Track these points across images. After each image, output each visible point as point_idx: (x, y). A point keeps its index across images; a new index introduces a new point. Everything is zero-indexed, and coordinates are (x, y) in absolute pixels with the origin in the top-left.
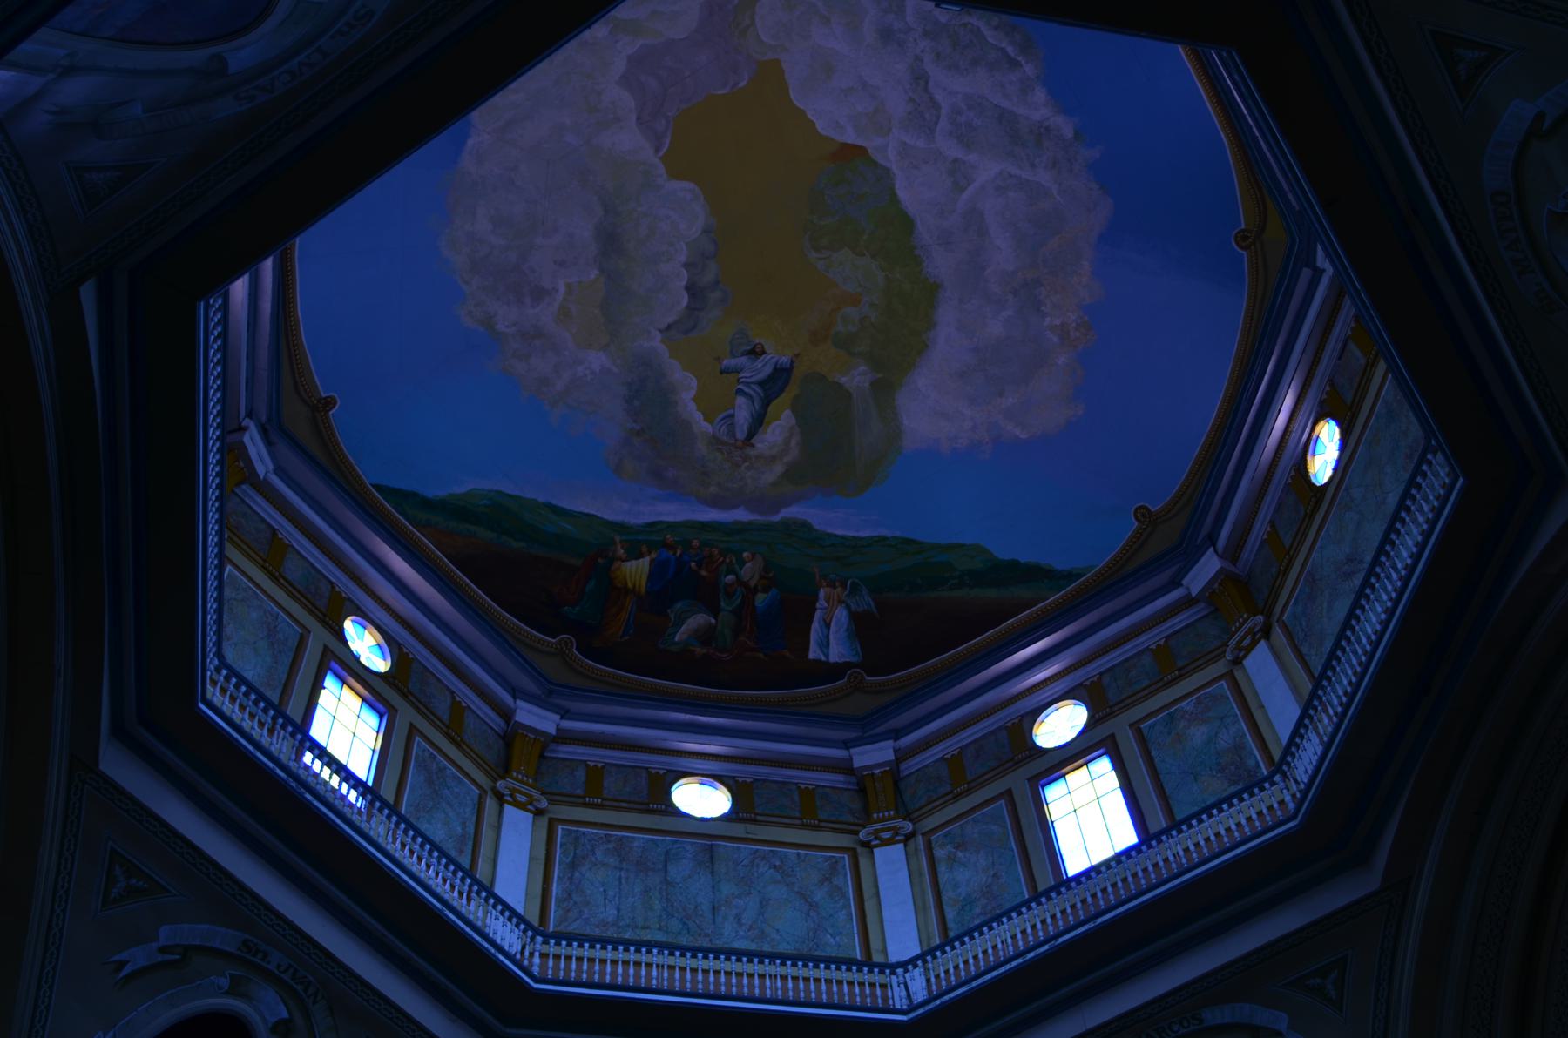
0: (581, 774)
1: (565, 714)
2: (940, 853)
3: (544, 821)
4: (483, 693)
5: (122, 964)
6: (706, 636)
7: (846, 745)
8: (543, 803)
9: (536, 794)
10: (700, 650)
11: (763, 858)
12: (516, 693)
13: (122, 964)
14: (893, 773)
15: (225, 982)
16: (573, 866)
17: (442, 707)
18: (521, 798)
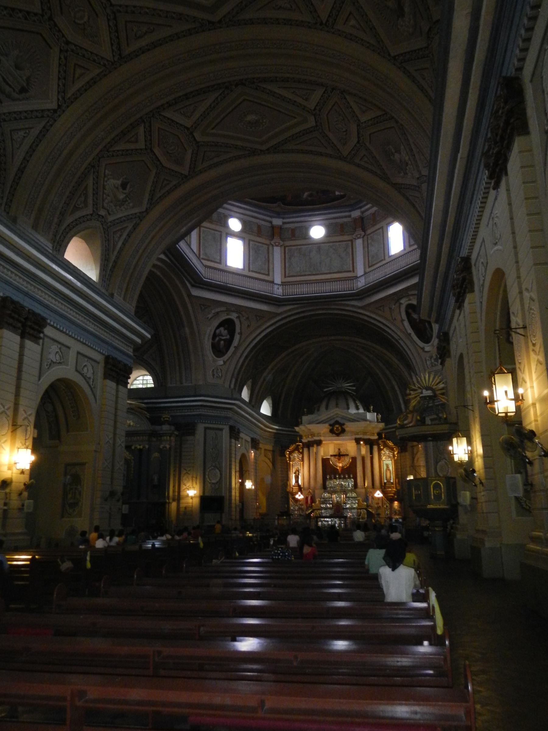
0: (290, 231)
1: (283, 218)
2: (369, 241)
3: (283, 248)
4: (264, 220)
5: (208, 318)
6: (310, 195)
7: (350, 211)
8: (282, 243)
9: (281, 242)
10: (309, 198)
11: (331, 247)
12: (271, 217)
13: (208, 318)
14: (362, 219)
15: (226, 314)
16: (290, 258)
17: (255, 229)
18: (277, 244)
